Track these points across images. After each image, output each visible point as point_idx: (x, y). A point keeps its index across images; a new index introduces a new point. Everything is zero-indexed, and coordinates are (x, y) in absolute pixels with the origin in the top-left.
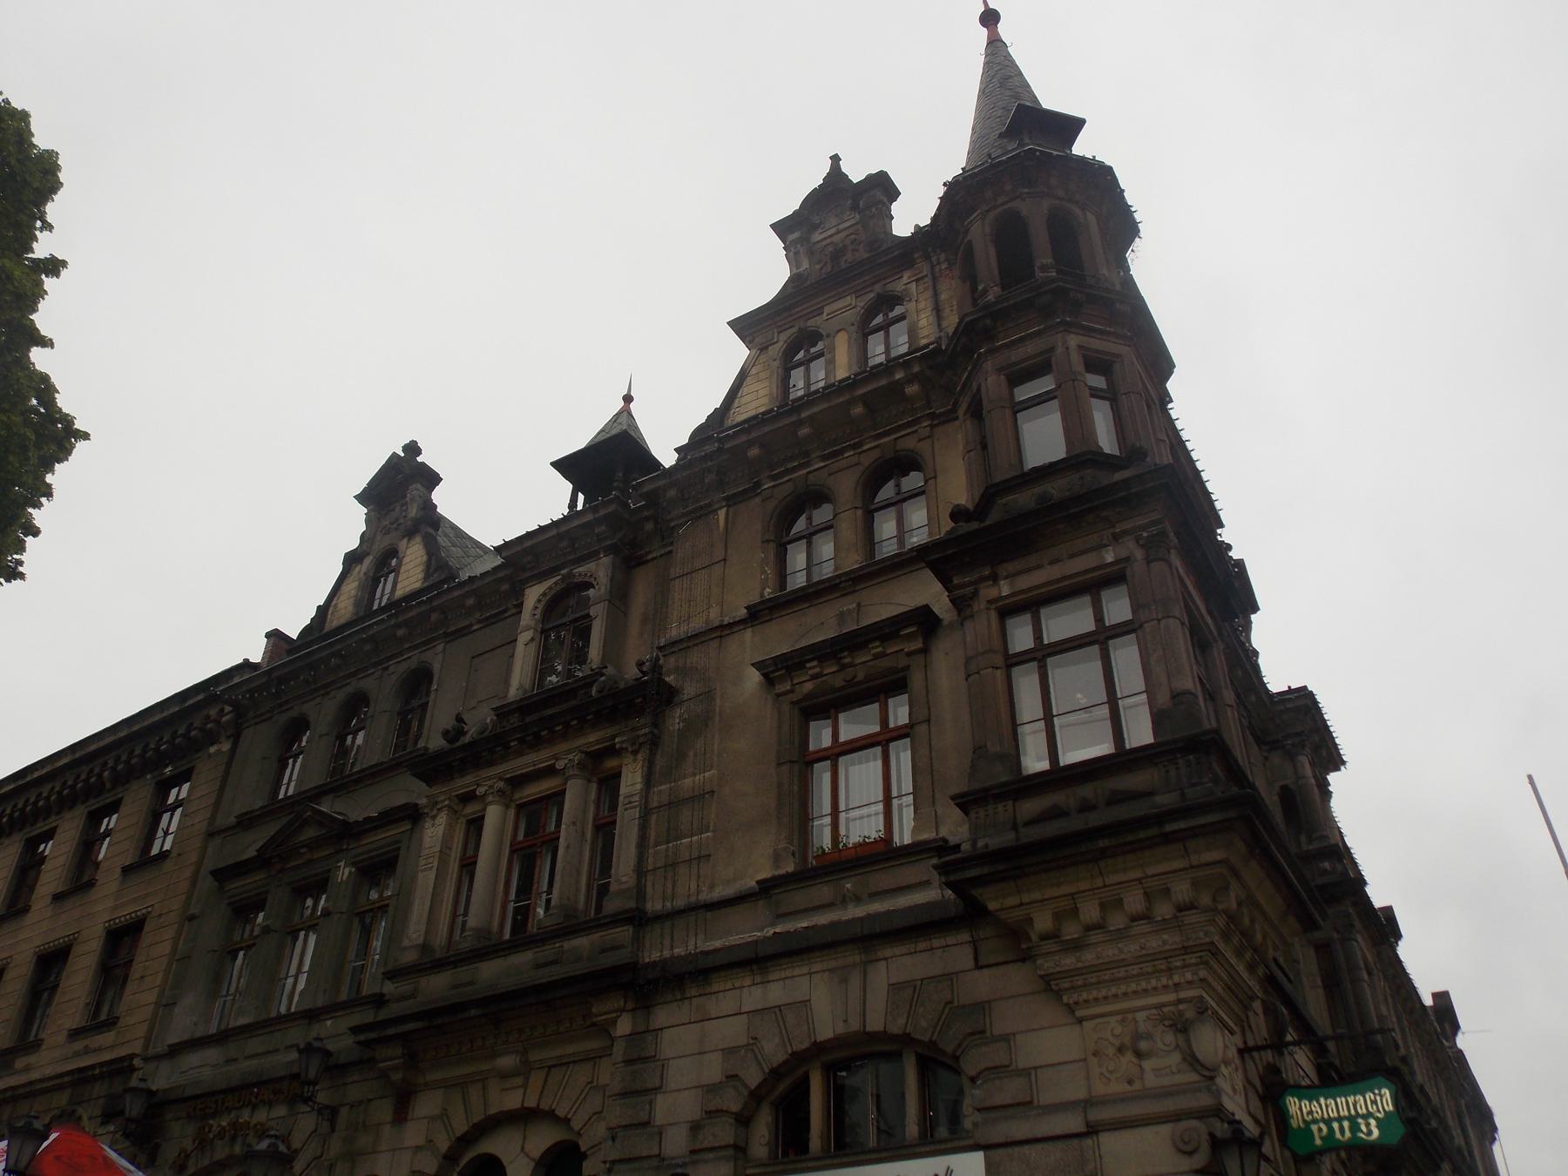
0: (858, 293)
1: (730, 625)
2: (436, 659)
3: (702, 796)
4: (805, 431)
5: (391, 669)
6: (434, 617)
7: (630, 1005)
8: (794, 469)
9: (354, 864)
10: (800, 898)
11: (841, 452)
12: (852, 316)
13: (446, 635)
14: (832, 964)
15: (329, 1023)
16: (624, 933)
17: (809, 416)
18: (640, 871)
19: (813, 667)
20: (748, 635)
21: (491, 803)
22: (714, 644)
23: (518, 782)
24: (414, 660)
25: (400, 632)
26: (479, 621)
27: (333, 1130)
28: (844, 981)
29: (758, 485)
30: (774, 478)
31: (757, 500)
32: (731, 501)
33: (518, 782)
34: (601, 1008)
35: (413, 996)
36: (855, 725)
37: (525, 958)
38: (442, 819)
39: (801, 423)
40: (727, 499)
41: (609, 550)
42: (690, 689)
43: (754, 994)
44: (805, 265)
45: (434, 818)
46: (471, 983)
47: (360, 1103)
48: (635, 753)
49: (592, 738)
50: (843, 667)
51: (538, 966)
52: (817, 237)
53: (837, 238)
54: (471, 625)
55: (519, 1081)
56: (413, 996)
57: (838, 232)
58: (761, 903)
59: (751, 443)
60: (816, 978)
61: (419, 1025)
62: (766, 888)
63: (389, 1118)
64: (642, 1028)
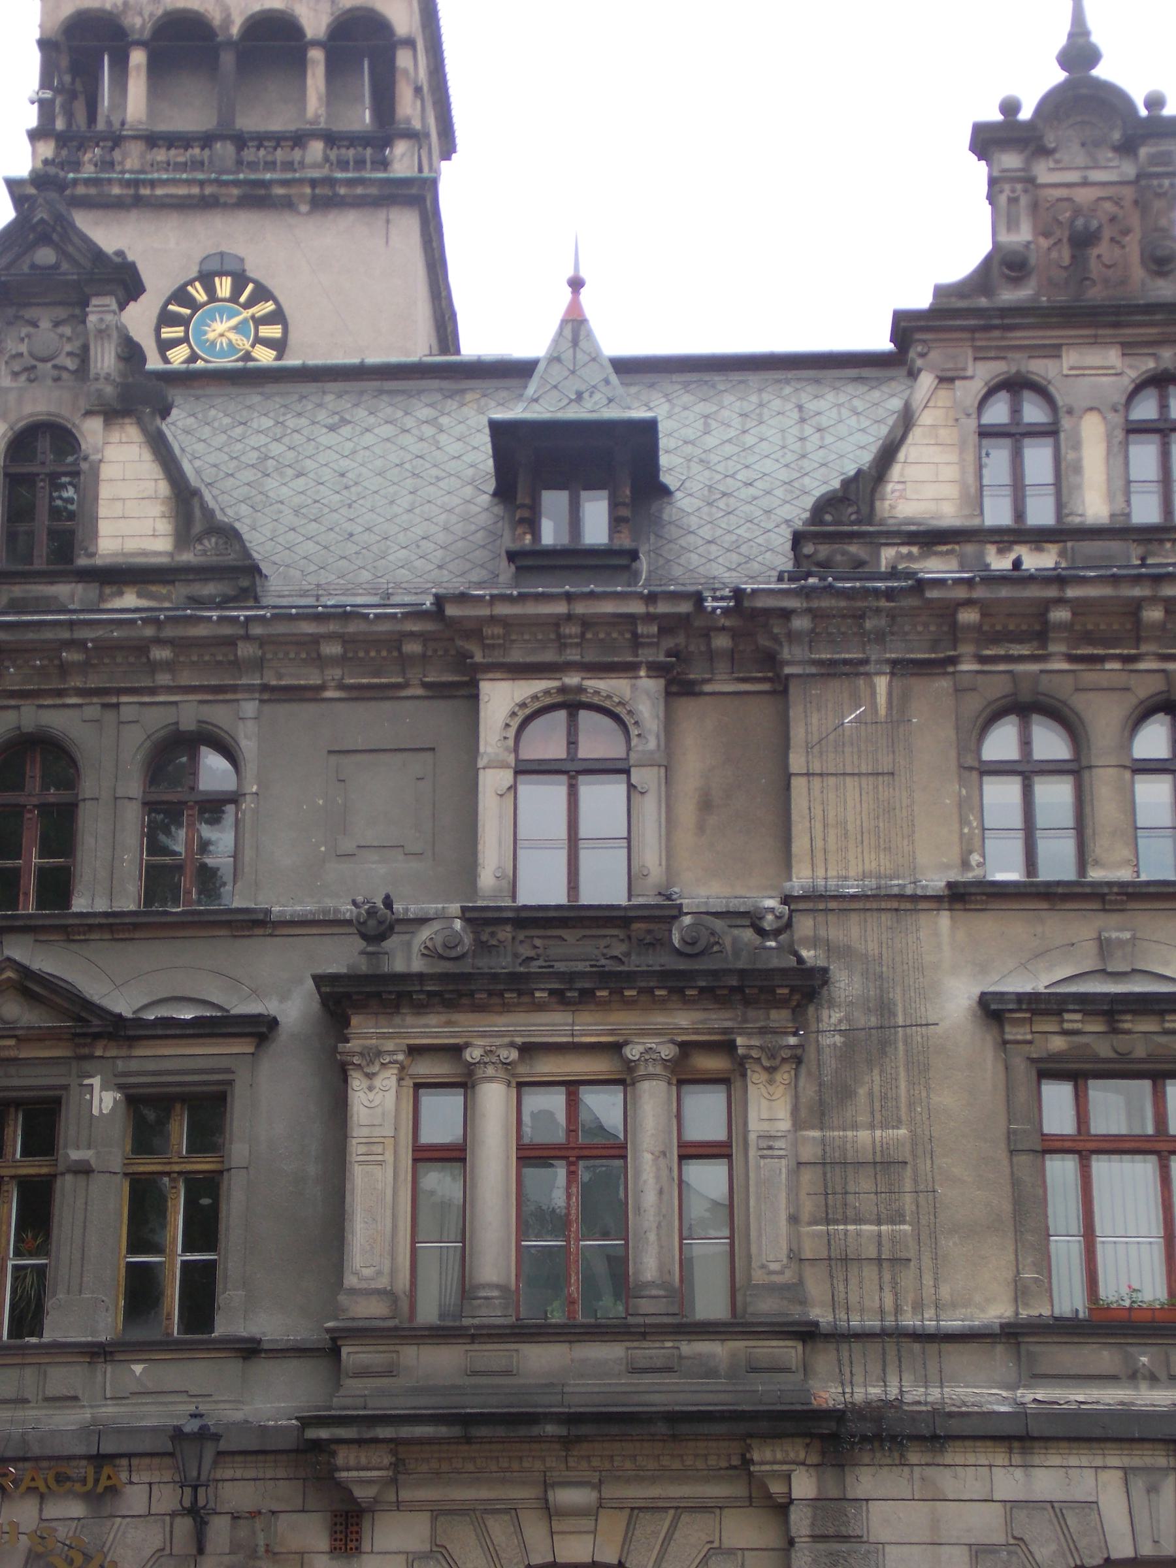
0: (1128, 348)
1: (914, 898)
2: (246, 723)
3: (886, 1165)
4: (1060, 615)
5: (127, 713)
6: (245, 650)
7: (814, 1459)
8: (1021, 659)
9: (120, 1087)
10: (1067, 1357)
11: (1101, 659)
12: (1116, 387)
13: (265, 688)
14: (1126, 1461)
15: (138, 1369)
16: (790, 1352)
17: (1077, 599)
18: (795, 1257)
19: (1073, 1020)
20: (944, 920)
21: (491, 1079)
22: (885, 918)
23: (528, 1050)
24: (190, 713)
25: (160, 654)
26: (342, 687)
27: (201, 1550)
28: (1152, 1489)
29: (953, 661)
30: (983, 660)
31: (944, 684)
32: (899, 668)
33: (528, 1050)
34: (764, 1456)
35: (389, 1372)
36: (1115, 1107)
37: (611, 1352)
38: (387, 1080)
39: (1061, 601)
40: (894, 663)
41: (656, 669)
42: (846, 984)
43: (1009, 1480)
44: (1024, 234)
45: (370, 1076)
46: (507, 1373)
47: (255, 1514)
48: (771, 1070)
49: (685, 1020)
50: (1115, 1031)
51: (635, 1370)
52: (1044, 172)
53: (1084, 196)
54: (322, 687)
55: (587, 1523)
56: (389, 1372)
57: (1085, 183)
58: (999, 1348)
59: (969, 603)
60: (1105, 1476)
61: (443, 1431)
62: (1012, 1334)
63: (324, 1544)
64: (833, 1493)
